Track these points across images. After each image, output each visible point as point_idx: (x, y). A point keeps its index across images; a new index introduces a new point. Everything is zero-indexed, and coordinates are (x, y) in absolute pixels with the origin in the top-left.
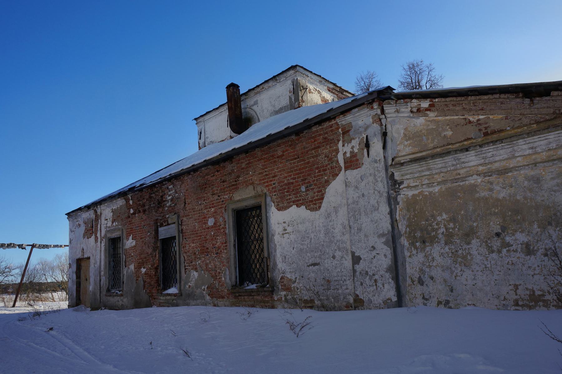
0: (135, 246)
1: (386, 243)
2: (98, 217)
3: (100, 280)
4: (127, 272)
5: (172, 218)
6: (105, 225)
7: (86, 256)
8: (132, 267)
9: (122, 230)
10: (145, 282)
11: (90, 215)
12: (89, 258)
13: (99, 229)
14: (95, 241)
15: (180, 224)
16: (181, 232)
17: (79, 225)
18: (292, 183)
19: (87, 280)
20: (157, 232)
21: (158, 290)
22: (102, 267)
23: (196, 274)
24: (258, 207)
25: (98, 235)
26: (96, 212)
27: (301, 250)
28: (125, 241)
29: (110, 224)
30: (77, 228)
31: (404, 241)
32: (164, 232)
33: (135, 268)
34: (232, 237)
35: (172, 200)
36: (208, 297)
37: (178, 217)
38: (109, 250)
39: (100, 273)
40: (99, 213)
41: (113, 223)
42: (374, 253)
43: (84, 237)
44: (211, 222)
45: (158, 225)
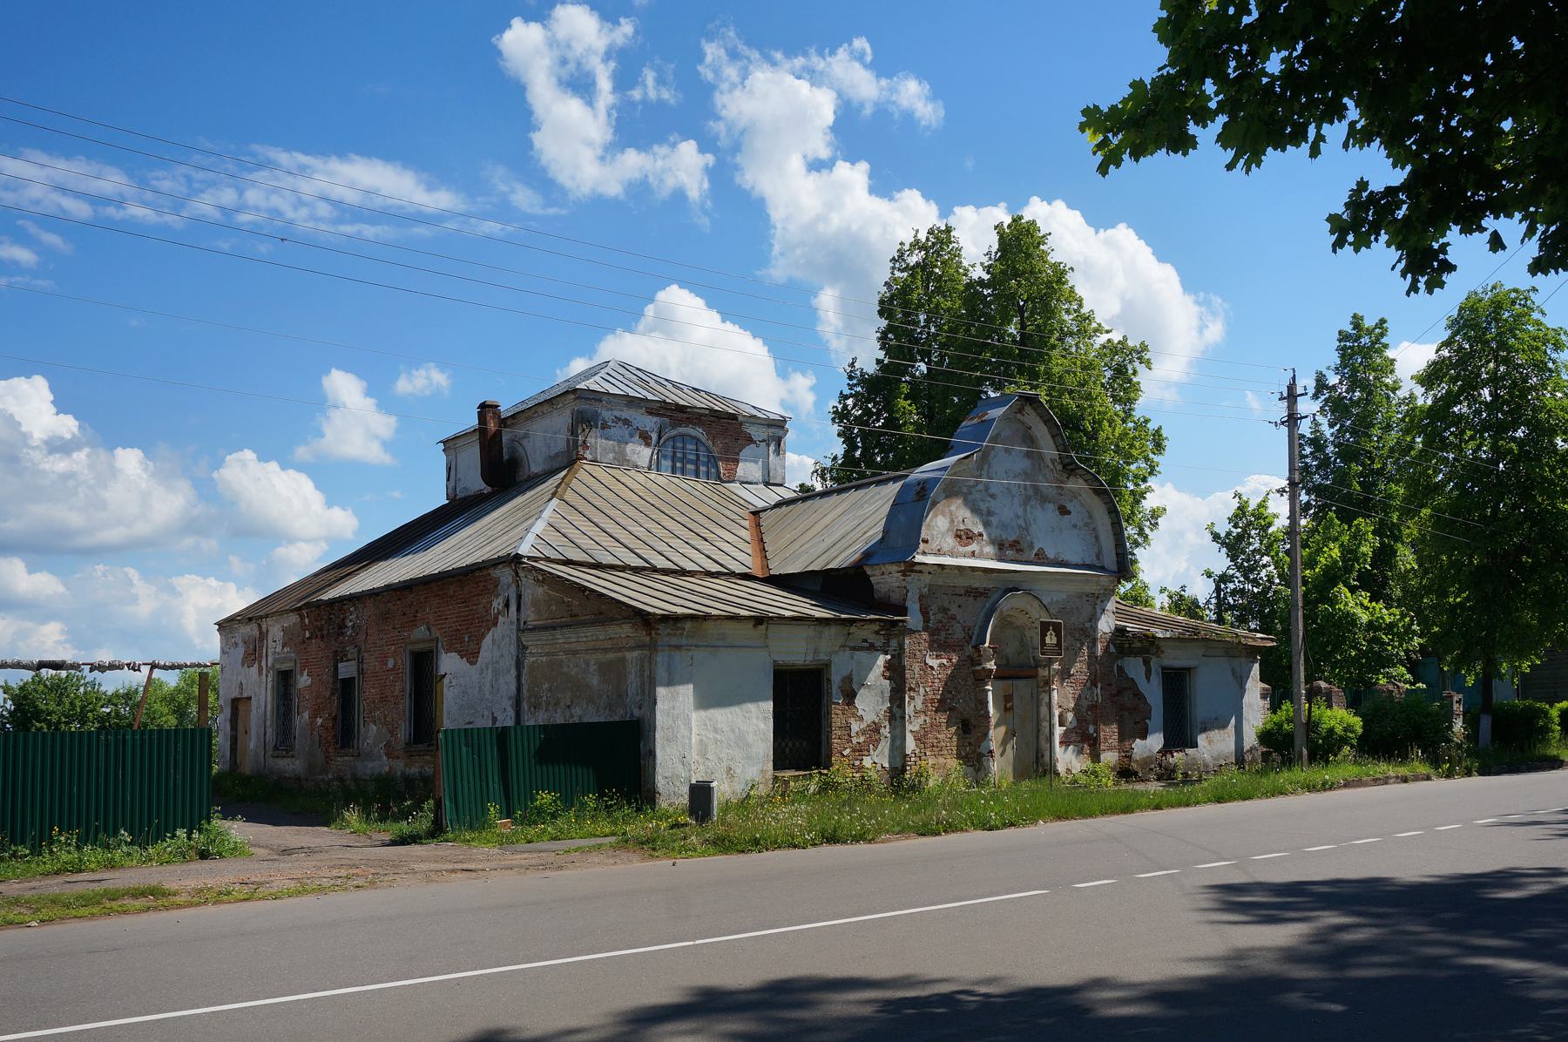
0: (310, 686)
1: (512, 706)
2: (263, 636)
3: (265, 734)
4: (300, 721)
5: (351, 651)
6: (273, 650)
7: (245, 695)
8: (306, 715)
9: (295, 660)
10: (320, 737)
11: (251, 630)
12: (249, 698)
13: (264, 654)
14: (259, 672)
15: (360, 661)
16: (361, 672)
17: (236, 644)
18: (459, 630)
19: (246, 733)
20: (336, 669)
21: (335, 748)
22: (268, 717)
23: (374, 728)
24: (432, 652)
25: (263, 663)
26: (260, 627)
27: (462, 706)
28: (298, 676)
29: (279, 649)
30: (232, 649)
31: (525, 706)
32: (347, 670)
33: (309, 718)
34: (408, 684)
35: (353, 627)
36: (385, 758)
37: (359, 651)
38: (278, 688)
39: (265, 722)
40: (264, 630)
41: (283, 647)
42: (505, 714)
43: (243, 665)
44: (391, 664)
45: (339, 657)
